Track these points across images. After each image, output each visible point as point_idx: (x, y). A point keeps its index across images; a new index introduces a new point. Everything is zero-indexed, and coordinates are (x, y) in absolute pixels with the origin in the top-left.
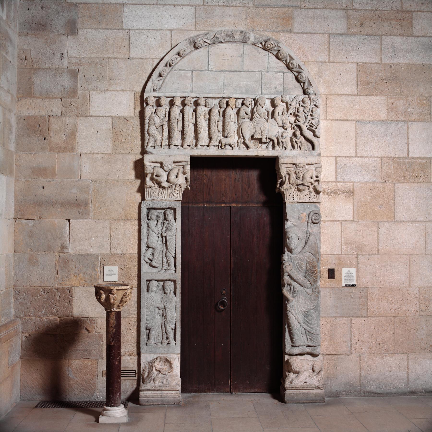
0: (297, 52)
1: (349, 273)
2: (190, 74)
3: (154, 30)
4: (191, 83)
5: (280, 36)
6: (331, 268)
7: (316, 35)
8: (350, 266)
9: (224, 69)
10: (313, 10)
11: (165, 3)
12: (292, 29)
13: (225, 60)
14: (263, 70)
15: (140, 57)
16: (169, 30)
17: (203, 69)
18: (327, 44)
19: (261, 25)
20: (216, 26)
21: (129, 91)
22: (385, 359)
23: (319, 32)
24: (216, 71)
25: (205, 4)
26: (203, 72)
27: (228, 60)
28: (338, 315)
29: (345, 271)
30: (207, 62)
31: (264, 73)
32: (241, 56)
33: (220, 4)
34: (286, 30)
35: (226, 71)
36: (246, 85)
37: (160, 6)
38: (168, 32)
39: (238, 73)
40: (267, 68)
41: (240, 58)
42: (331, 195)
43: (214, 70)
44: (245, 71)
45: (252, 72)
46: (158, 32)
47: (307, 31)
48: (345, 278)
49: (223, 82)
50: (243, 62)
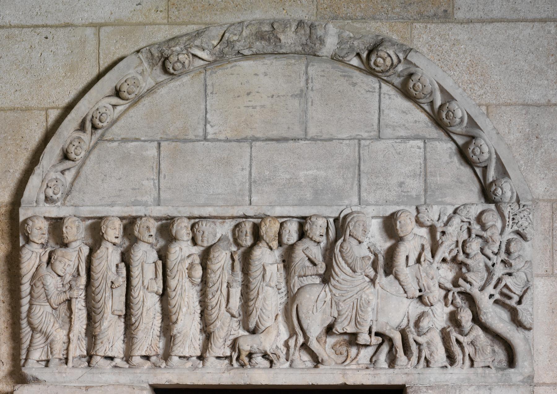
0: (466, 77)
2: (152, 151)
3: (51, 27)
5: (415, 32)
7: (521, 25)
9: (249, 133)
12: (450, 10)
13: (254, 108)
14: (365, 135)
16: (91, 25)
17: (191, 136)
20: (226, 8)
23: (530, 16)
24: (227, 140)
26: (190, 145)
27: (263, 106)
30: (202, 114)
31: (368, 142)
32: (302, 95)
35: (257, 139)
36: (316, 179)
38: (90, 31)
39: (291, 143)
40: (376, 127)
41: (296, 102)
43: (222, 137)
44: (313, 139)
45: (331, 140)
46: (61, 33)
47: (496, 14)
49: (246, 172)
50: (305, 112)
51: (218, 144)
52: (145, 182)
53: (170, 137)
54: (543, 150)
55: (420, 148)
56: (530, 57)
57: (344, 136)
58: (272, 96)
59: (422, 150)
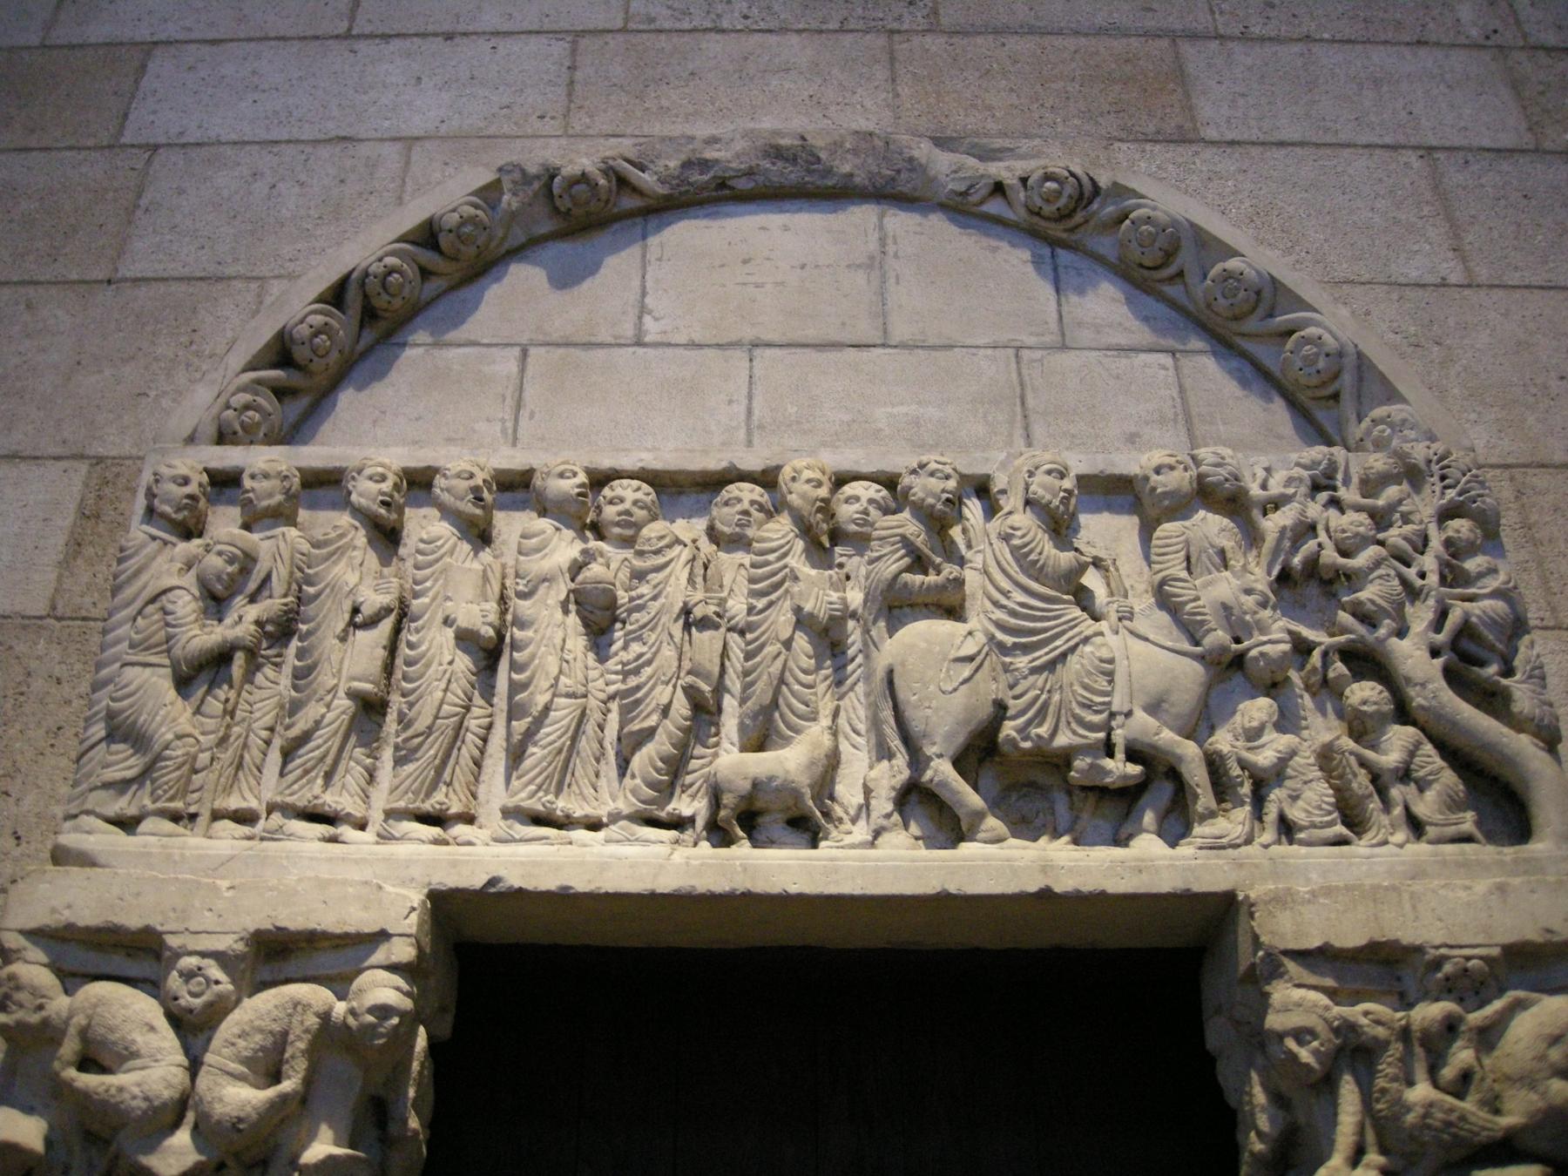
2: (507, 363)
4: (509, 416)
7: (1346, 152)
9: (748, 333)
10: (1296, 48)
11: (397, 28)
12: (1188, 125)
15: (186, 272)
17: (604, 336)
18: (1428, 196)
19: (990, 108)
21: (57, 458)
25: (631, 26)
30: (633, 296)
31: (1038, 354)
33: (725, 24)
34: (1151, 128)
35: (769, 345)
36: (916, 422)
37: (362, 46)
40: (1054, 325)
41: (860, 278)
43: (682, 338)
49: (740, 409)
50: (882, 294)
51: (669, 351)
52: (481, 426)
53: (555, 337)
54: (1458, 368)
55: (1165, 368)
56: (1380, 204)
57: (980, 342)
58: (803, 267)
59: (1171, 372)
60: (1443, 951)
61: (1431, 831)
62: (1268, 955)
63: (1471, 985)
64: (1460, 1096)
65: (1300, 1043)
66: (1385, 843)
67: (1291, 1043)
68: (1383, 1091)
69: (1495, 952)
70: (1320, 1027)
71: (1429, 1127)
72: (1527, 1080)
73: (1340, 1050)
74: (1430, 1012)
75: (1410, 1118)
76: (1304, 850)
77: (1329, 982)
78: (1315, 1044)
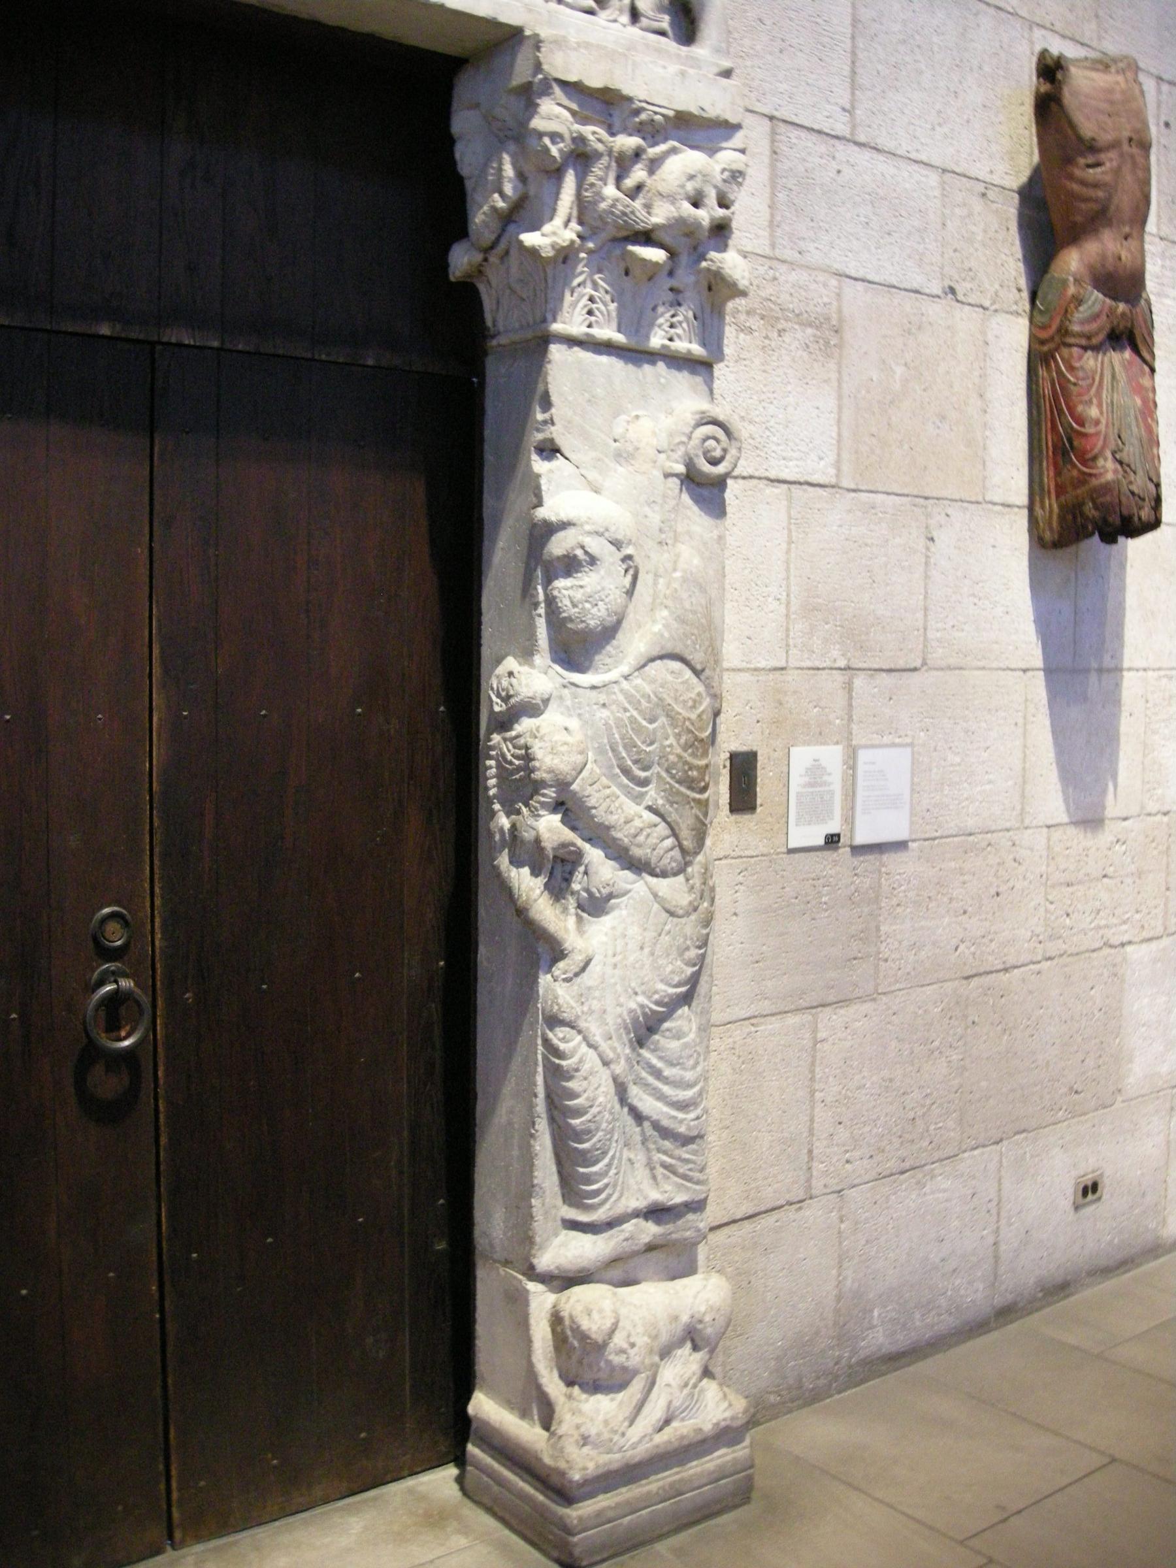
1: (816, 771)
6: (744, 749)
8: (820, 737)
22: (927, 1189)
28: (766, 1006)
29: (802, 757)
42: (750, 331)
48: (799, 803)
60: (644, 105)
61: (644, 22)
62: (545, 78)
63: (652, 131)
64: (633, 198)
65: (554, 143)
66: (615, 21)
67: (547, 141)
68: (592, 185)
69: (671, 113)
70: (567, 136)
71: (612, 213)
72: (671, 198)
73: (572, 152)
74: (627, 142)
75: (603, 206)
76: (568, 11)
77: (574, 107)
78: (562, 145)
